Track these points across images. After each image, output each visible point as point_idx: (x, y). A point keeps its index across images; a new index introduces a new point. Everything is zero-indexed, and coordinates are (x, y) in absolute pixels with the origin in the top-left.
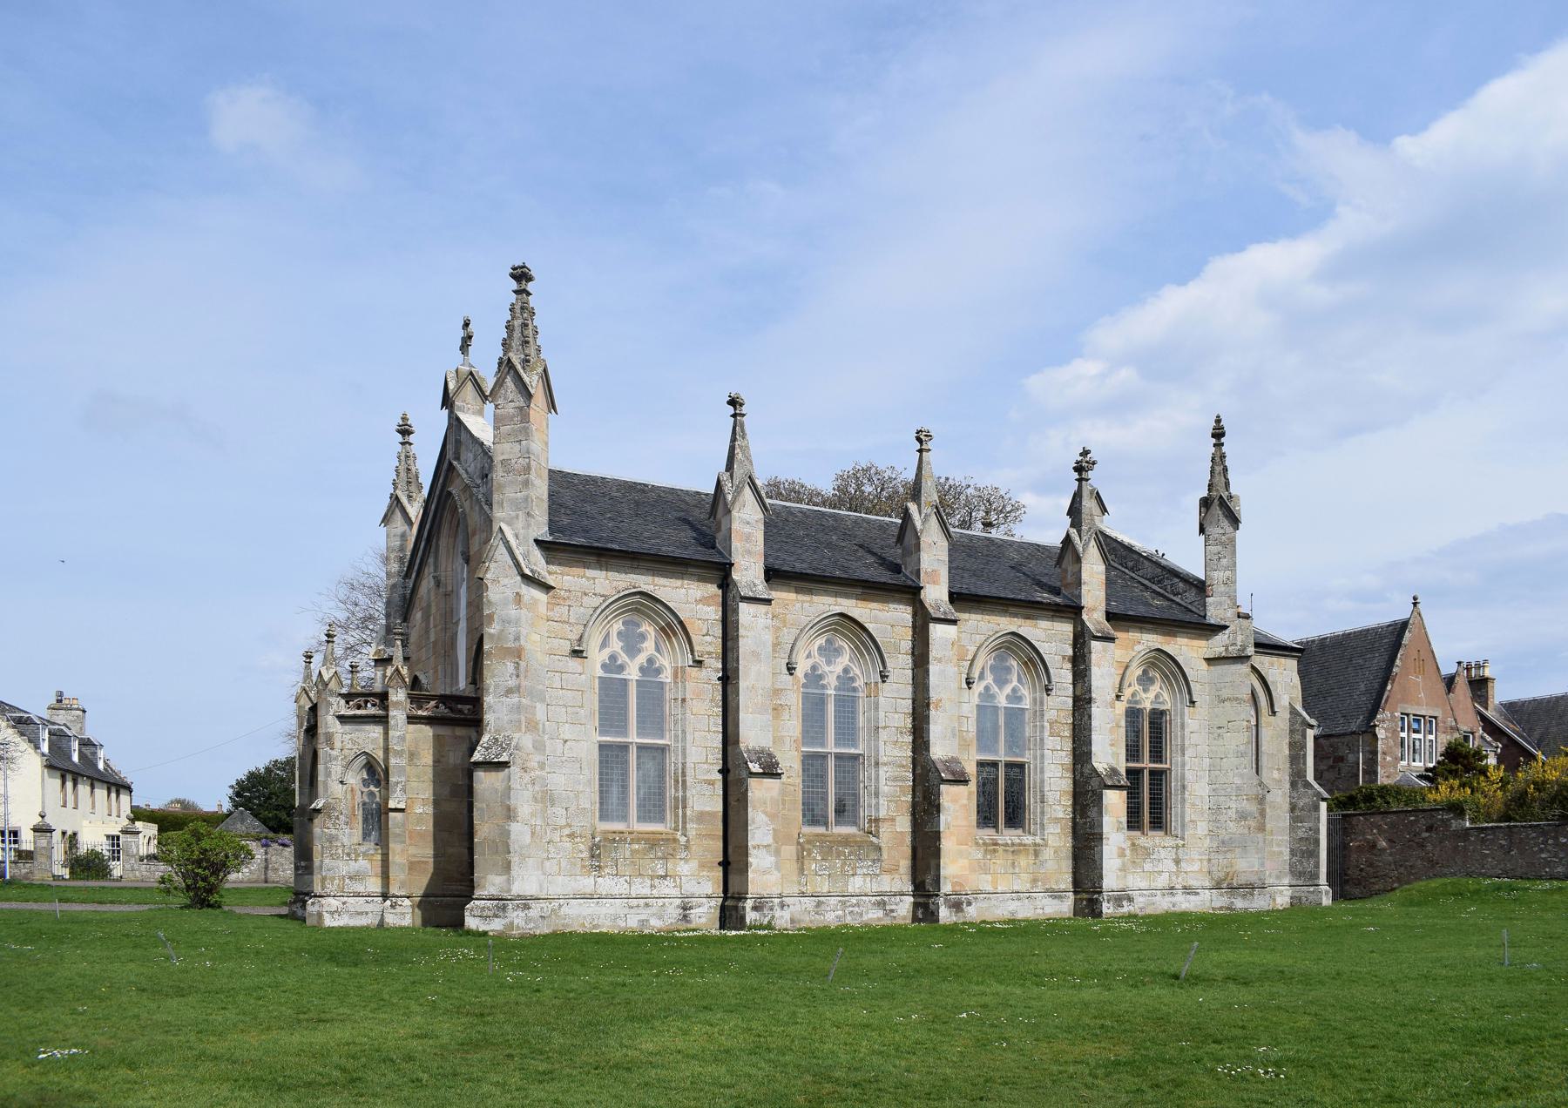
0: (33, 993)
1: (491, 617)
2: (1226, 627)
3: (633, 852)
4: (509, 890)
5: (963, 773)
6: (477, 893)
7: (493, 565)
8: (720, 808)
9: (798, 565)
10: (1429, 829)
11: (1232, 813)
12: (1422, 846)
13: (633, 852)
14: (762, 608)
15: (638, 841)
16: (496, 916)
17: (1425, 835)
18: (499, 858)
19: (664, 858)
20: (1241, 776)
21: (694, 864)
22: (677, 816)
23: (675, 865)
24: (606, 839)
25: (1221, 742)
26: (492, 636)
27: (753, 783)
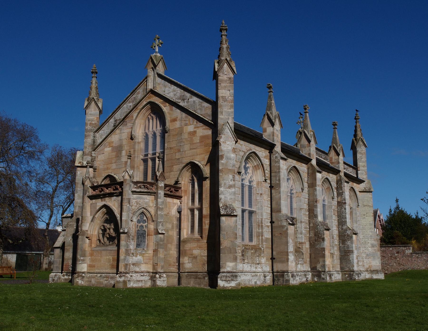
0: (92, 314)
1: (222, 156)
2: (364, 181)
3: (252, 253)
4: (236, 269)
5: (233, 210)
6: (222, 270)
7: (223, 136)
8: (270, 237)
9: (199, 111)
10: (398, 253)
11: (369, 244)
12: (396, 258)
13: (252, 253)
14: (371, 193)
15: (252, 249)
16: (232, 280)
17: (396, 255)
18: (231, 255)
19: (258, 256)
20: (372, 232)
21: (265, 259)
22: (259, 239)
23: (261, 259)
24: (245, 248)
25: (365, 220)
26: (223, 164)
27: (223, 219)
